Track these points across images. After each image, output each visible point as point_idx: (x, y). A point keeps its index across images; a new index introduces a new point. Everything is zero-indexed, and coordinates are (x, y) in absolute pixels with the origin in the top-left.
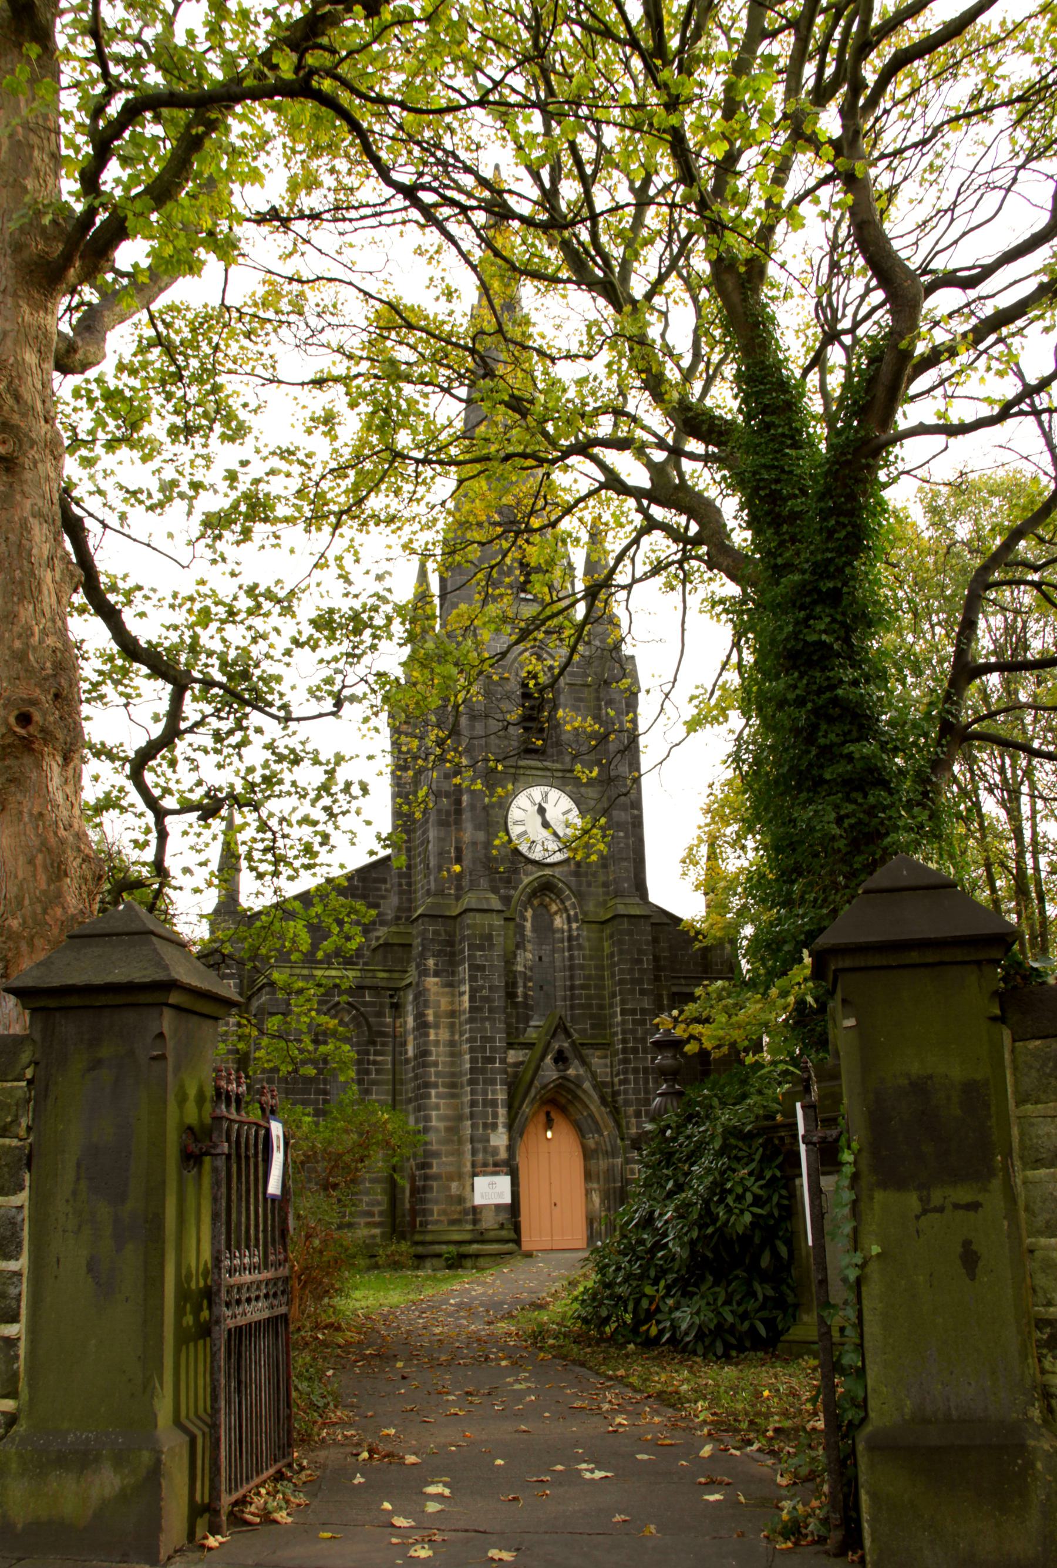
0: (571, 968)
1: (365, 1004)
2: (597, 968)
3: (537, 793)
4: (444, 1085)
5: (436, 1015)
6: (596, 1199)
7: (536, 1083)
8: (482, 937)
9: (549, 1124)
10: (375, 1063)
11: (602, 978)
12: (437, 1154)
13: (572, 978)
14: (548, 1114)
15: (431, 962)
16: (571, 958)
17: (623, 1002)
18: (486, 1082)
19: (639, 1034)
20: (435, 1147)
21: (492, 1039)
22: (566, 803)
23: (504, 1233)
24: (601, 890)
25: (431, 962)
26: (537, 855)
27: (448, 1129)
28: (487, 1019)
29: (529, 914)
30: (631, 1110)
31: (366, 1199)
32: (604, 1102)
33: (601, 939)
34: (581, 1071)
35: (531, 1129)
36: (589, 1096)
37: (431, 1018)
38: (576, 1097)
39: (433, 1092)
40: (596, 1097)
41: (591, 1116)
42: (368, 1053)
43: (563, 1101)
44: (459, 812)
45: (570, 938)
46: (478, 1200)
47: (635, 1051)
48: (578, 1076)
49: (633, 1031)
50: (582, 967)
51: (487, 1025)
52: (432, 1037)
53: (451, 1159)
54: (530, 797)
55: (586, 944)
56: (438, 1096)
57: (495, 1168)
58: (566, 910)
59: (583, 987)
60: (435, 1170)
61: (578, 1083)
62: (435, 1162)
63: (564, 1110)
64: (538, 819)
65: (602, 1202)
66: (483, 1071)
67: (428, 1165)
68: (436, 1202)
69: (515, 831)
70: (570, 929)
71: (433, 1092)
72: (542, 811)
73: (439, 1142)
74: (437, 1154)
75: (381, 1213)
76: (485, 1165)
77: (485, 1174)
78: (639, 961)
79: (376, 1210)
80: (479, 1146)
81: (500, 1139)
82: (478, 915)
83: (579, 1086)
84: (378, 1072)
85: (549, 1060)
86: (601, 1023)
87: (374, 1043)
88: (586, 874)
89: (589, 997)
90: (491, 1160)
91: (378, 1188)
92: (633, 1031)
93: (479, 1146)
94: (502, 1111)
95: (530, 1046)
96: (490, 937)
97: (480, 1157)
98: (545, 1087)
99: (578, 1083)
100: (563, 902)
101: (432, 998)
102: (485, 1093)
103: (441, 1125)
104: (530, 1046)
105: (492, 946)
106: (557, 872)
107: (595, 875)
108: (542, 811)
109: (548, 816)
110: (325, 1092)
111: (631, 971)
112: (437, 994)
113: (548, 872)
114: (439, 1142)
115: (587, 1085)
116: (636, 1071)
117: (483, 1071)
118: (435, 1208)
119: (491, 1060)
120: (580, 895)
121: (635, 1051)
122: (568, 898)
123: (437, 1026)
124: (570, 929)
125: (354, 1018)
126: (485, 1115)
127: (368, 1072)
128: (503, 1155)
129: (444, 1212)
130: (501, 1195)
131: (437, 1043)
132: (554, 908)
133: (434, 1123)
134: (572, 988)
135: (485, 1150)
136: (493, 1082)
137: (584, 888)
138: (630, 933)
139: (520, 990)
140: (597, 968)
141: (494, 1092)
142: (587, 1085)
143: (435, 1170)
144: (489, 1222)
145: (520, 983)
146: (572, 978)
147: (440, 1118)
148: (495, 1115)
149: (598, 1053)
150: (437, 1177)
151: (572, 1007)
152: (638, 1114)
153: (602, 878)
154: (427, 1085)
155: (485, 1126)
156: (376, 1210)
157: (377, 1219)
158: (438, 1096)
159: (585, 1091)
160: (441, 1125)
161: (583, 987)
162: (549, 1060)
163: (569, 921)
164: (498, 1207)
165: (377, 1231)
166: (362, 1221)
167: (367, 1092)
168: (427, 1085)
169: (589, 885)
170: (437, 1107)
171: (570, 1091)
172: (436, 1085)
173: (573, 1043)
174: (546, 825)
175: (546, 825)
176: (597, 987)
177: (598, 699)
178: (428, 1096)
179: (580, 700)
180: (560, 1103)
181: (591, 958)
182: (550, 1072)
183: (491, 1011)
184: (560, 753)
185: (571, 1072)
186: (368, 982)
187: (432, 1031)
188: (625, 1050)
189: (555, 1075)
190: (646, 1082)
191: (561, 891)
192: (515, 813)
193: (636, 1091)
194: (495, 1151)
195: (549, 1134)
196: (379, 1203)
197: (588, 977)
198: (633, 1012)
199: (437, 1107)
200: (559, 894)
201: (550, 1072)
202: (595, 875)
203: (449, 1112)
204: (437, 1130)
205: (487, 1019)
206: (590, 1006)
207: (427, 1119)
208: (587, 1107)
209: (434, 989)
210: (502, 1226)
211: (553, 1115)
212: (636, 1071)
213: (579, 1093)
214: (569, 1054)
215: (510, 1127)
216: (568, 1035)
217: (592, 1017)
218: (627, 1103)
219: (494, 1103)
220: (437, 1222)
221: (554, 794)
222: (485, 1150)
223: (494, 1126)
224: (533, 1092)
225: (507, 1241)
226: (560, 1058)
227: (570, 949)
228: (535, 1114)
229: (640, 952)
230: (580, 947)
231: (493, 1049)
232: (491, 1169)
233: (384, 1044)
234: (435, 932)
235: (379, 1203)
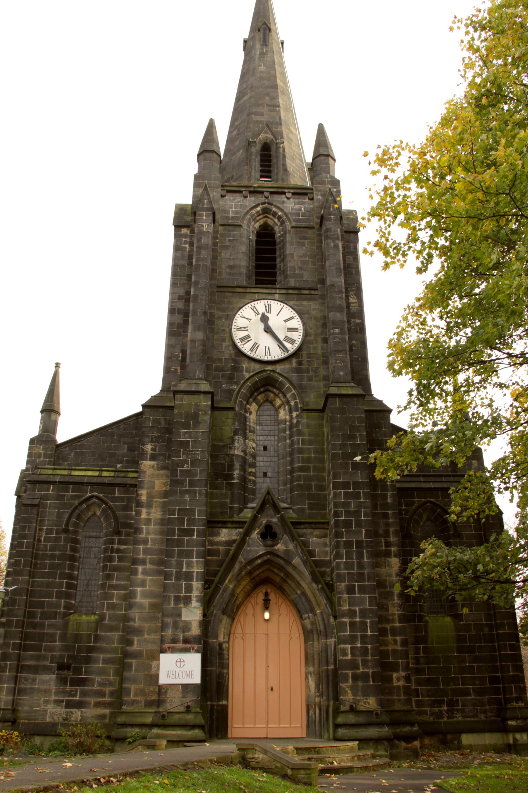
0: (291, 454)
1: (114, 499)
2: (316, 451)
3: (260, 306)
4: (152, 562)
5: (149, 495)
6: (312, 684)
7: (241, 558)
8: (188, 416)
9: (266, 606)
10: (118, 551)
11: (322, 461)
12: (139, 631)
13: (292, 462)
14: (266, 594)
15: (149, 447)
16: (292, 443)
17: (335, 477)
18: (181, 554)
19: (352, 508)
20: (137, 624)
21: (192, 512)
22: (288, 312)
23: (190, 718)
24: (322, 384)
25: (149, 447)
26: (260, 354)
27: (153, 606)
28: (187, 492)
29: (253, 407)
30: (343, 586)
31: (98, 679)
32: (315, 579)
33: (321, 426)
34: (291, 547)
35: (249, 609)
36: (300, 573)
37: (144, 498)
38: (288, 575)
39: (140, 568)
40: (306, 573)
41: (304, 594)
42: (112, 542)
43: (278, 580)
44: (186, 322)
45: (291, 427)
46: (163, 680)
47: (347, 524)
48: (287, 552)
49: (346, 505)
50: (301, 451)
51: (187, 497)
52: (144, 516)
53: (153, 636)
54: (254, 310)
55: (306, 430)
56: (144, 573)
57: (185, 645)
58: (288, 402)
59: (301, 469)
60: (135, 647)
61: (287, 558)
62: (136, 639)
63: (281, 590)
64: (262, 326)
65: (317, 686)
66: (179, 543)
67: (130, 643)
68: (135, 681)
69: (238, 335)
70: (292, 418)
71: (140, 568)
72: (264, 319)
73: (142, 619)
74: (139, 631)
75: (112, 694)
76: (174, 641)
77: (174, 651)
78: (354, 437)
79: (107, 690)
80: (169, 620)
81: (192, 615)
82: (185, 397)
83: (288, 562)
84: (120, 559)
85: (255, 535)
86: (319, 503)
87: (119, 533)
88: (308, 371)
89: (306, 479)
90: (181, 636)
91: (112, 668)
92: (346, 505)
93: (170, 620)
94: (197, 585)
95: (239, 524)
96: (196, 416)
97: (169, 632)
98: (251, 562)
99: (287, 558)
100: (285, 396)
101: (147, 479)
102: (180, 565)
103: (146, 602)
104: (239, 524)
105: (197, 424)
106: (279, 368)
107: (316, 371)
108: (264, 319)
109: (270, 323)
110: (70, 577)
111: (343, 446)
112: (153, 475)
113: (269, 368)
114: (142, 619)
115: (297, 561)
116: (348, 544)
117: (179, 543)
118: (133, 688)
119: (189, 532)
120: (301, 389)
121: (347, 524)
122: (289, 390)
123: (149, 505)
124: (292, 418)
125: (104, 511)
126: (178, 588)
127: (110, 559)
128: (195, 631)
129: (142, 692)
130: (189, 674)
131: (148, 521)
132: (278, 402)
133: (138, 599)
134: (292, 471)
135: (175, 626)
136: (189, 554)
137: (305, 382)
138: (342, 411)
139: (236, 473)
140: (316, 451)
141: (189, 565)
142: (297, 561)
143: (135, 647)
144: (174, 703)
145: (237, 466)
146: (292, 462)
147: (145, 595)
148: (189, 589)
149: (317, 532)
150: (137, 655)
151: (292, 490)
152: (350, 590)
153: (322, 372)
154: (135, 561)
155: (177, 599)
156: (107, 690)
157: (107, 699)
158: (144, 573)
159: (295, 568)
160: (146, 602)
161: (301, 469)
162: (255, 535)
163: (291, 412)
164: (185, 687)
165: (107, 711)
166: (92, 700)
167: (109, 577)
168: (135, 561)
169: (310, 379)
170: (143, 584)
171: (281, 568)
172: (143, 562)
173: (282, 519)
174: (268, 330)
175: (268, 330)
176: (316, 469)
177: (320, 235)
178: (135, 572)
179: (305, 238)
180: (269, 579)
181: (311, 443)
182: (256, 547)
183: (191, 484)
184: (286, 277)
185: (280, 547)
186: (118, 481)
187: (144, 510)
188: (337, 523)
189: (262, 550)
190: (360, 556)
191: (282, 384)
192: (239, 321)
193: (349, 566)
194: (187, 626)
195: (267, 615)
196: (111, 684)
197: (309, 460)
198: (346, 485)
199: (143, 584)
200: (279, 387)
201: (256, 547)
202: (316, 371)
203: (156, 589)
204: (141, 606)
205: (187, 492)
206: (309, 487)
207: (132, 595)
208: (299, 585)
209: (149, 471)
210: (188, 709)
211: (272, 596)
212: (348, 544)
213: (290, 569)
214: (278, 529)
215: (207, 603)
216: (277, 509)
217: (310, 497)
218: (340, 578)
219: (188, 576)
220: (133, 702)
221: (276, 306)
222: (175, 626)
223: (187, 600)
224: (237, 567)
225: (194, 727)
226: (269, 534)
227: (291, 436)
228: (248, 595)
229: (352, 428)
230: (300, 433)
231: (191, 522)
232: (181, 645)
233: (128, 534)
234: (154, 420)
235: (111, 684)
